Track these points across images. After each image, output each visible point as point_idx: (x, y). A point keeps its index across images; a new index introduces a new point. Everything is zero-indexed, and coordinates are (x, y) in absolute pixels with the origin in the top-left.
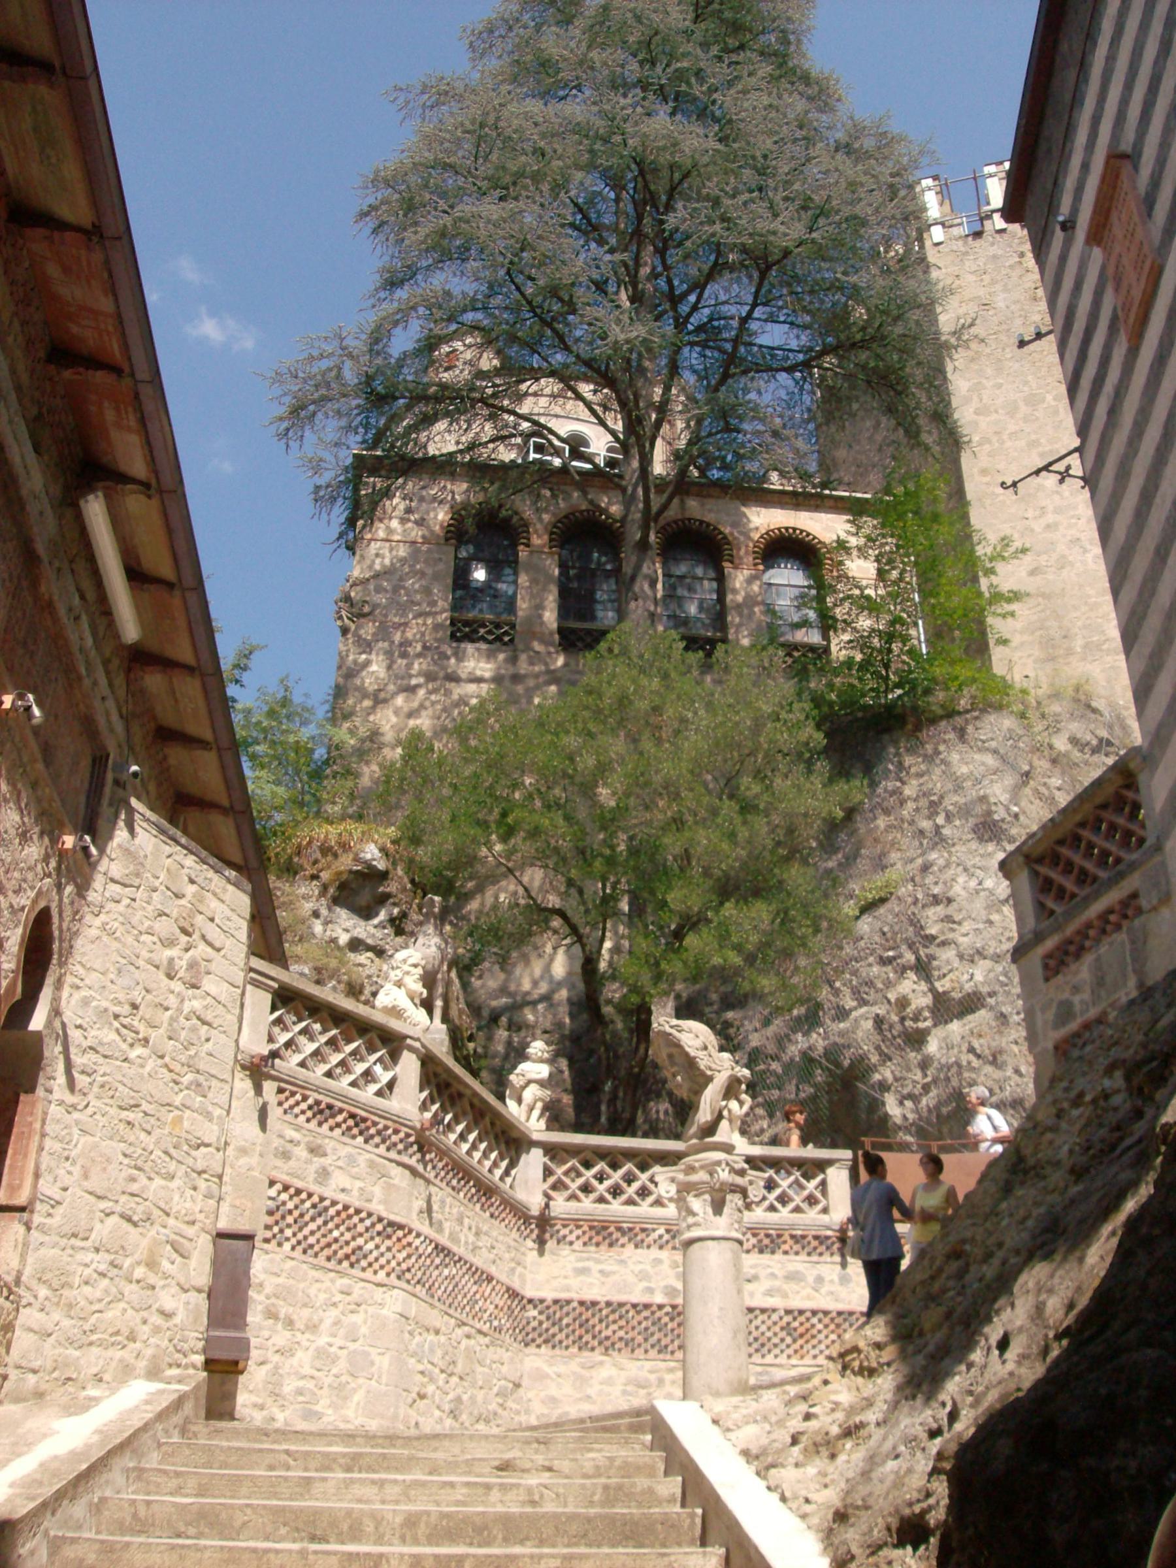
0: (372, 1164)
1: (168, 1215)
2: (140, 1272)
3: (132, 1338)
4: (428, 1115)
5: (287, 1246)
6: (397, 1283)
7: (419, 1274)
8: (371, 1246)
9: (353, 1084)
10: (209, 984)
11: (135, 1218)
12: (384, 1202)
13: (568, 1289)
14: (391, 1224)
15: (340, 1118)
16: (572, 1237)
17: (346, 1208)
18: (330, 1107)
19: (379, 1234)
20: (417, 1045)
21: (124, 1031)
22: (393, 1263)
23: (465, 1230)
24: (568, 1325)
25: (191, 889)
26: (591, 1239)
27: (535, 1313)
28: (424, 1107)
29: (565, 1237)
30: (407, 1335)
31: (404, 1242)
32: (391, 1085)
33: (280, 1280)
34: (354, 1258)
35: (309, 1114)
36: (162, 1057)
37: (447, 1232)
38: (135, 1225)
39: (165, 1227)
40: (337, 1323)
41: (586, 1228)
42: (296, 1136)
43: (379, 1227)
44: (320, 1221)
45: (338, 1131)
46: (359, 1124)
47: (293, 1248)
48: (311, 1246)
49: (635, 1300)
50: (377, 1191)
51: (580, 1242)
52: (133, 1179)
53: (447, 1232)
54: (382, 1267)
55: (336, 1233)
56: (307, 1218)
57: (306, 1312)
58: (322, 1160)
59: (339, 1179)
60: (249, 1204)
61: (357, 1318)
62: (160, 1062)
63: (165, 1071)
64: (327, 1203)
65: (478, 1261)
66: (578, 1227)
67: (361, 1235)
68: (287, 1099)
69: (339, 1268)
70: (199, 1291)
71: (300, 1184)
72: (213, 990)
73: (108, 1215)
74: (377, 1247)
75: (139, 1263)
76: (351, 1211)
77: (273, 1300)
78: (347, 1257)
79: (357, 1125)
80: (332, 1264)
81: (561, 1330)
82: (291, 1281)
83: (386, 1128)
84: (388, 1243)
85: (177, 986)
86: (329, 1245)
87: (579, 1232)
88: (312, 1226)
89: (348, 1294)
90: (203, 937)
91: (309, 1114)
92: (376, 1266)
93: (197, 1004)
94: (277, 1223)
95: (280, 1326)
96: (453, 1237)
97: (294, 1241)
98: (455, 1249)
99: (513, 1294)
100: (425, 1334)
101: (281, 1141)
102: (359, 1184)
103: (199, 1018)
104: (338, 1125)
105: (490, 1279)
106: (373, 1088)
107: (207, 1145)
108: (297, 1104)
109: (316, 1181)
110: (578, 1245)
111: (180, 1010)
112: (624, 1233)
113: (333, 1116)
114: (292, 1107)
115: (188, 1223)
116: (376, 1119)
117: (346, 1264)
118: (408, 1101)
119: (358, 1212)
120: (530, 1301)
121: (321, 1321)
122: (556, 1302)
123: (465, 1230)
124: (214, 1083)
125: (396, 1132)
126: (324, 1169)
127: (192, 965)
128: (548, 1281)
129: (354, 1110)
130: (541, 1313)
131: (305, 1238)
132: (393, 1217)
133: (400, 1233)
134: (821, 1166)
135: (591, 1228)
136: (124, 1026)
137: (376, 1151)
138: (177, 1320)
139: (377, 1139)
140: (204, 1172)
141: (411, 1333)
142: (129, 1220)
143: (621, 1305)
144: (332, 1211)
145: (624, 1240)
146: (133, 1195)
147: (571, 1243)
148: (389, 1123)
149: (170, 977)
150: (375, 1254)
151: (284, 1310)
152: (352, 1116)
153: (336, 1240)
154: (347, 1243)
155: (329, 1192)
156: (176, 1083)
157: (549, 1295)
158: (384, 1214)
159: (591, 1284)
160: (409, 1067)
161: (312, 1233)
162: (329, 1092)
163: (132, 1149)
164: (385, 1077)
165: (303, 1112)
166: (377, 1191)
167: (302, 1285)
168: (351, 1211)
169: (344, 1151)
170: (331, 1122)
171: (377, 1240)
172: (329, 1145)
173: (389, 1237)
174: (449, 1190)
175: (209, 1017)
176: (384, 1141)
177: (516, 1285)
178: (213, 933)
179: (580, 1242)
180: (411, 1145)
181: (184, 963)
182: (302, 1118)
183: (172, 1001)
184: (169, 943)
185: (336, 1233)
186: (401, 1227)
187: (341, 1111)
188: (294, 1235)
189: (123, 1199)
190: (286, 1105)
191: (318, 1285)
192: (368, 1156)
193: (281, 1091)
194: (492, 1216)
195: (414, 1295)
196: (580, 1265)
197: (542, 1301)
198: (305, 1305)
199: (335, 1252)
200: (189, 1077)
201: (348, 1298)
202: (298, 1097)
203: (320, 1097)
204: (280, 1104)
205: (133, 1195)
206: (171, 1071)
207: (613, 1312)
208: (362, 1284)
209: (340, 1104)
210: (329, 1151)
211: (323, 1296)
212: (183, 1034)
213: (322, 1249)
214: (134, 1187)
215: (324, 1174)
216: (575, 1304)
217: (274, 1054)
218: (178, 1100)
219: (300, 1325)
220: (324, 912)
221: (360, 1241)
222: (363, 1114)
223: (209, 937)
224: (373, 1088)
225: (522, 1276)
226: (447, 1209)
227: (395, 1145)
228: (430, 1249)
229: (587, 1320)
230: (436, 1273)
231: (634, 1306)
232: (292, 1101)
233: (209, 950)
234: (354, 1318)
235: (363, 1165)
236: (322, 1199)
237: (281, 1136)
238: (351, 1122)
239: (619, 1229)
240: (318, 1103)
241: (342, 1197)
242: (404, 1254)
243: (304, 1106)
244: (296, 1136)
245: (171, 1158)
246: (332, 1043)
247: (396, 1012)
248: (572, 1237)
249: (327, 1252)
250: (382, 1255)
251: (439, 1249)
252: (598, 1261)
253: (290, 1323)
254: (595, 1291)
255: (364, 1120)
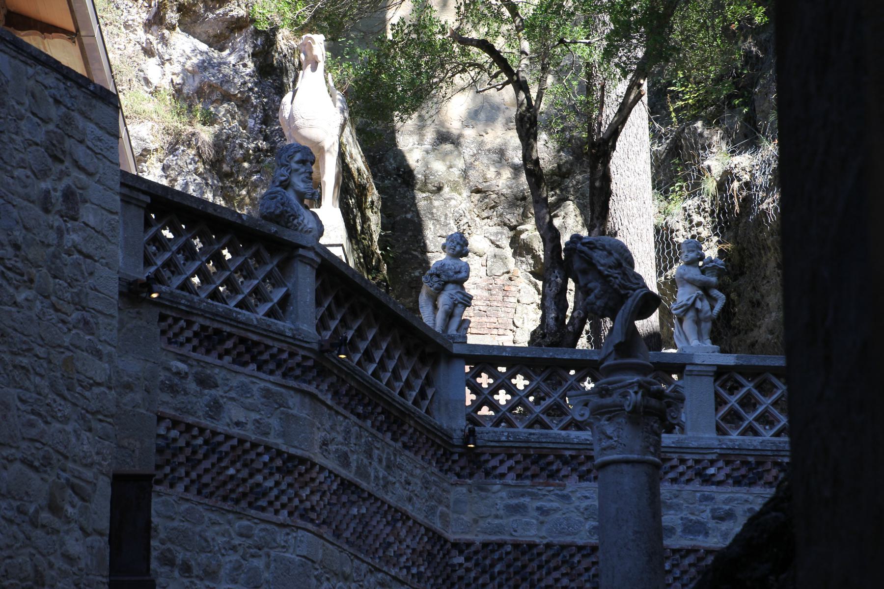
1: (66, 458)
4: (327, 335)
5: (180, 488)
6: (300, 523)
7: (325, 513)
8: (270, 483)
9: (242, 305)
10: (88, 215)
11: (36, 464)
12: (283, 435)
13: (499, 530)
14: (291, 457)
15: (229, 344)
16: (503, 469)
17: (241, 441)
18: (218, 332)
19: (279, 469)
20: (311, 255)
21: (10, 274)
22: (296, 502)
23: (375, 463)
24: (500, 573)
26: (526, 469)
27: (461, 560)
29: (495, 468)
30: (314, 581)
31: (307, 477)
32: (285, 301)
33: (176, 524)
34: (254, 498)
35: (195, 342)
36: (47, 297)
37: (354, 465)
38: (36, 469)
39: (64, 471)
40: (238, 568)
41: (519, 457)
42: (182, 366)
43: (279, 462)
44: (214, 458)
45: (227, 359)
46: (249, 351)
47: (187, 489)
48: (206, 485)
49: (580, 542)
50: (274, 423)
51: (512, 475)
52: (31, 425)
53: (354, 465)
54: (283, 506)
55: (232, 471)
56: (200, 456)
57: (203, 558)
58: (213, 392)
59: (236, 413)
60: (138, 445)
61: (259, 563)
62: (47, 302)
63: (52, 311)
64: (220, 438)
65: (389, 498)
66: (510, 456)
67: (259, 471)
68: (170, 326)
69: (237, 509)
70: (101, 534)
71: (190, 420)
72: (91, 220)
73: (11, 461)
74: (277, 484)
75: (42, 508)
76: (248, 445)
77: (169, 545)
78: (244, 495)
79: (248, 350)
80: (227, 506)
81: (492, 578)
82: (186, 524)
83: (281, 351)
84: (289, 479)
85: (57, 221)
86: (225, 483)
87: (511, 462)
88: (207, 464)
89: (248, 537)
90: (76, 164)
91: (195, 342)
92: (278, 505)
93: (75, 237)
94: (168, 462)
95: (176, 574)
96: (362, 471)
97: (187, 481)
98: (364, 485)
99: (436, 538)
100: (334, 581)
101: (168, 374)
102: (255, 416)
103: (80, 252)
104: (227, 352)
105: (406, 517)
107: (99, 384)
108: (182, 329)
109: (208, 416)
110: (510, 479)
111: (59, 245)
112: (566, 462)
113: (222, 342)
114: (176, 335)
115: (86, 466)
116: (270, 343)
117: (244, 504)
119: (254, 445)
120: (455, 545)
121: (219, 566)
122: (485, 545)
123: (375, 463)
124: (101, 319)
125: (292, 355)
126: (216, 402)
128: (476, 521)
129: (243, 333)
130: (467, 559)
131: (199, 476)
132: (292, 451)
133: (303, 468)
135: (526, 456)
136: (9, 269)
137: (272, 378)
138: (82, 565)
139: (272, 366)
140: (98, 412)
141: (318, 578)
142: (31, 465)
143: (563, 547)
144: (225, 448)
145: (566, 470)
146: (32, 440)
147: (502, 476)
148: (285, 346)
149: (47, 211)
150: (275, 492)
151: (180, 556)
152: (243, 340)
153: (232, 477)
154: (244, 480)
155: (221, 427)
156: (64, 322)
157: (479, 539)
158: (284, 448)
159: (527, 523)
161: (206, 471)
162: (215, 316)
163: (28, 395)
164: (277, 295)
165: (188, 340)
167: (198, 529)
168: (248, 445)
169: (235, 381)
170: (220, 349)
171: (277, 477)
172: (219, 374)
173: (290, 472)
174: (354, 418)
175: (89, 249)
176: (279, 366)
177: (438, 526)
179: (512, 475)
180: (310, 369)
181: (59, 194)
182: (189, 347)
184: (42, 174)
185: (232, 471)
186: (302, 460)
187: (230, 335)
188: (187, 474)
189: (24, 445)
190: (171, 334)
191: (217, 528)
192: (263, 384)
193: (163, 318)
194: (405, 446)
195: (321, 537)
196: (514, 501)
197: (469, 544)
198: (203, 550)
199: (232, 491)
200: (75, 315)
201: (250, 542)
202: (182, 323)
203: (207, 323)
204: (163, 332)
205: (32, 440)
206: (57, 310)
207: (554, 556)
208: (263, 526)
209: (228, 329)
210: (220, 382)
211: (220, 540)
212: (66, 271)
213: (217, 488)
214: (33, 433)
215: (216, 408)
216: (509, 548)
218: (67, 340)
219: (196, 571)
221: (259, 478)
222: (255, 338)
223: (82, 162)
224: (265, 308)
225: (443, 516)
226: (353, 441)
227: (292, 369)
228: (335, 487)
229: (524, 567)
230: (343, 511)
231: (580, 548)
232: (176, 329)
233: (83, 176)
234: (256, 562)
235: (257, 395)
236: (214, 433)
237: (168, 369)
238: (242, 348)
239: (559, 457)
240: (204, 328)
241: (235, 431)
242: (308, 491)
243: (189, 334)
244: (182, 366)
245: (65, 399)
248: (503, 469)
249: (221, 492)
250: (283, 492)
251: (346, 485)
252: (534, 496)
253: (186, 569)
254: (530, 530)
255: (256, 344)
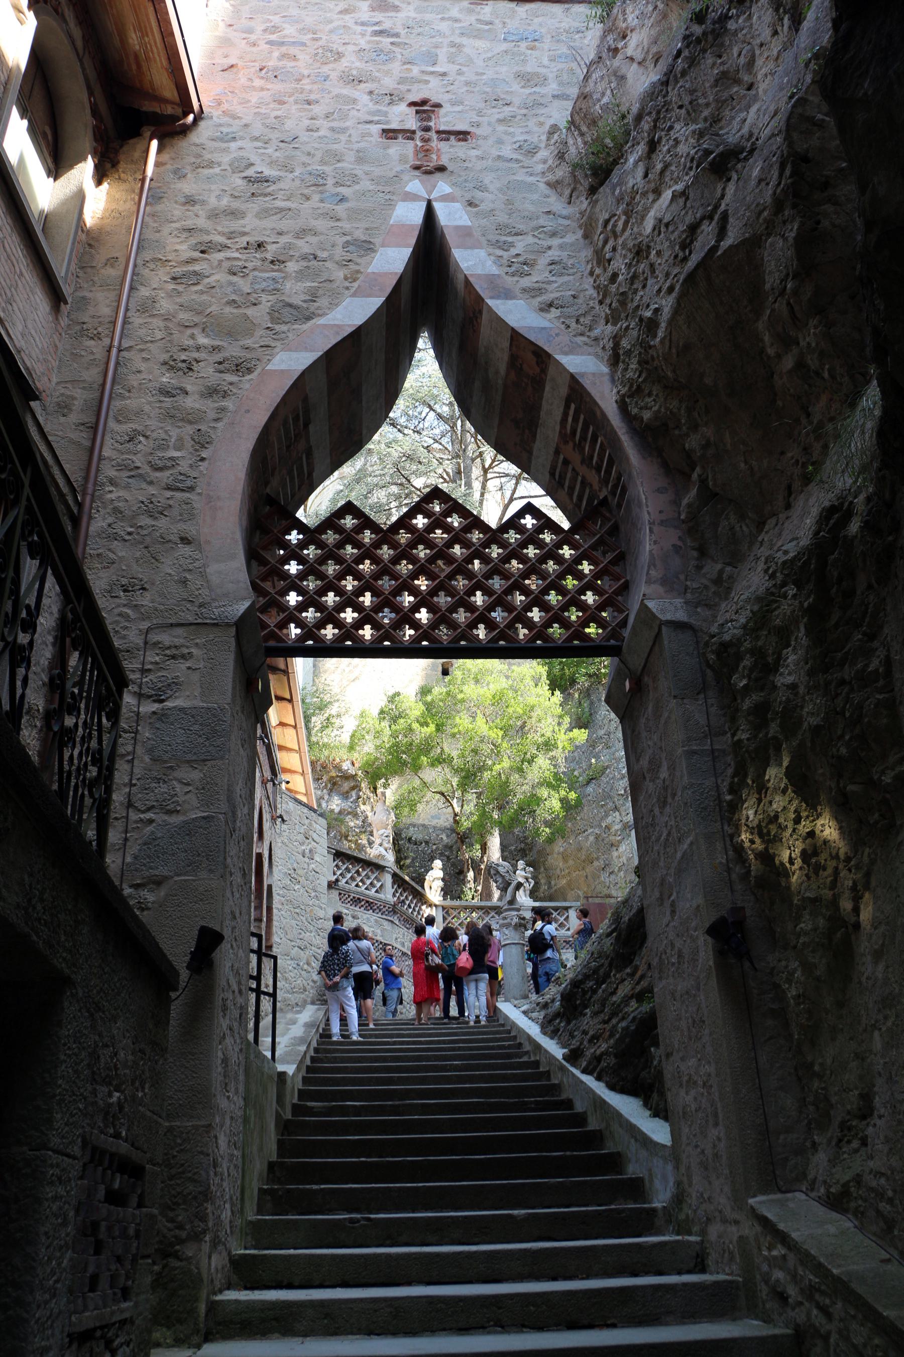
0: (376, 921)
2: (306, 967)
3: (305, 990)
25: (307, 822)
28: (394, 895)
46: (370, 905)
106: (374, 890)
118: (389, 894)
127: (311, 851)
134: (567, 909)
160: (388, 879)
162: (358, 893)
164: (378, 885)
166: (379, 931)
169: (365, 916)
172: (359, 914)
178: (315, 836)
183: (306, 866)
217: (337, 880)
220: (326, 797)
224: (374, 890)
246: (358, 872)
247: (380, 856)
